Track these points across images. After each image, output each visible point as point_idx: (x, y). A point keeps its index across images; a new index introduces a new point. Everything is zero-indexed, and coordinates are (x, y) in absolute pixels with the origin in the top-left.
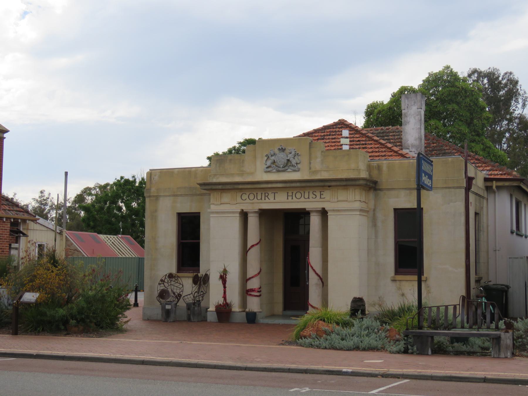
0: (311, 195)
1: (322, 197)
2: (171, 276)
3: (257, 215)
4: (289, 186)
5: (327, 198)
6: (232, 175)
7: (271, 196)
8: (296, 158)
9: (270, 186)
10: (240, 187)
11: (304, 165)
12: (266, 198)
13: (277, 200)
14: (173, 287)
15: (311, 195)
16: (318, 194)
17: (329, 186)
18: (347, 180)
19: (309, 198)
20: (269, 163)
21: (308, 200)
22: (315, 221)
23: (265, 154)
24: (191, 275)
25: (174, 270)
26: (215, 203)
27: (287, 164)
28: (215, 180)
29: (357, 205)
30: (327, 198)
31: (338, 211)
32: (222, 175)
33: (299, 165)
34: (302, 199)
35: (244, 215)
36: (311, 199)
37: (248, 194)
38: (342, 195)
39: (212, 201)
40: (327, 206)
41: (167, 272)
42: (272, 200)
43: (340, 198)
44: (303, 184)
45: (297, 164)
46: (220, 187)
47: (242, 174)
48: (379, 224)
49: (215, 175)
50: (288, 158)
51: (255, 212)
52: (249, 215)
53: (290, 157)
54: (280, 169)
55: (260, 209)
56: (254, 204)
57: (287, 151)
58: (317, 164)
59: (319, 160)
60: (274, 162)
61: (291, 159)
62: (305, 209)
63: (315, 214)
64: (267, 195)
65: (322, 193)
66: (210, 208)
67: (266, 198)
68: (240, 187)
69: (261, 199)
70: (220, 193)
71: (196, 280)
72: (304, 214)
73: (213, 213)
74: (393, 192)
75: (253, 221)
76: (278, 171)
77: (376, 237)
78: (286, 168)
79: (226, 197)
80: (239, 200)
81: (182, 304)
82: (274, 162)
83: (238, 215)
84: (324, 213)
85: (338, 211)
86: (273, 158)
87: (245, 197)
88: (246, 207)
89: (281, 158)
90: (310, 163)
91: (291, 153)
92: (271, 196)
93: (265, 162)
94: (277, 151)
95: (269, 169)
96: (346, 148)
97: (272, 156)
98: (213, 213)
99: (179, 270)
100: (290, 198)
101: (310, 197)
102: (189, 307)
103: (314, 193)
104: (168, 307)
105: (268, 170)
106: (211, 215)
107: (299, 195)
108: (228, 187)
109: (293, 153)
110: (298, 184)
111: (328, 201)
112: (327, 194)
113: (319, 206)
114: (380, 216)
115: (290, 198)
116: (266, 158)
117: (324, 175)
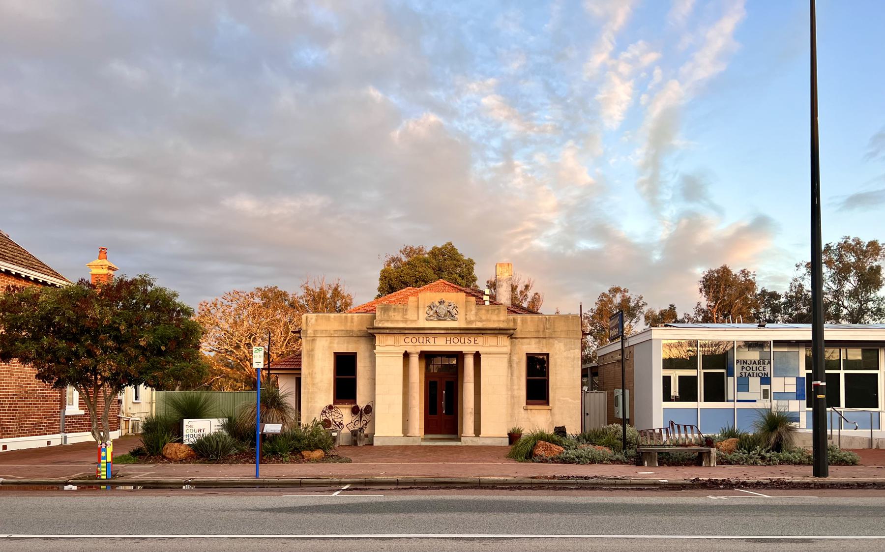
0: (467, 341)
2: (330, 407)
4: (449, 332)
6: (397, 321)
7: (432, 340)
9: (433, 332)
10: (406, 332)
11: (461, 316)
14: (332, 417)
15: (467, 341)
16: (472, 340)
18: (500, 329)
20: (431, 313)
22: (469, 362)
24: (350, 406)
25: (332, 403)
28: (380, 325)
32: (388, 321)
35: (406, 355)
38: (492, 340)
40: (481, 350)
41: (328, 404)
42: (432, 343)
44: (462, 332)
47: (406, 321)
48: (515, 365)
49: (381, 321)
53: (450, 309)
55: (422, 352)
56: (416, 346)
57: (446, 304)
58: (472, 316)
59: (473, 312)
68: (406, 332)
71: (355, 411)
72: (460, 356)
74: (525, 340)
75: (415, 361)
77: (512, 375)
79: (390, 340)
80: (403, 343)
81: (345, 431)
84: (477, 356)
89: (442, 310)
92: (432, 340)
96: (487, 303)
99: (335, 403)
102: (354, 433)
104: (334, 434)
108: (395, 331)
110: (458, 332)
112: (480, 340)
113: (474, 349)
114: (515, 358)
117: (479, 325)
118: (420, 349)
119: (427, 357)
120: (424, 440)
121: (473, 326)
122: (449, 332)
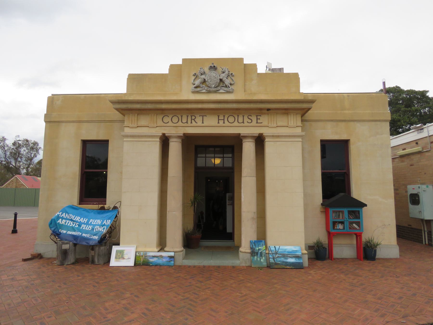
0: (246, 119)
1: (259, 121)
3: (180, 140)
5: (265, 123)
8: (229, 78)
12: (193, 121)
13: (205, 124)
17: (268, 110)
19: (243, 122)
21: (242, 124)
22: (249, 148)
23: (194, 73)
26: (130, 125)
27: (219, 84)
29: (298, 131)
30: (265, 123)
31: (278, 136)
33: (232, 87)
34: (236, 124)
35: (165, 141)
36: (246, 124)
37: (171, 116)
38: (281, 120)
39: (126, 124)
40: (265, 131)
42: (200, 123)
43: (279, 124)
45: (231, 84)
46: (138, 106)
50: (221, 77)
51: (179, 137)
52: (171, 140)
53: (223, 76)
54: (211, 89)
55: (184, 134)
57: (220, 70)
60: (205, 80)
61: (224, 79)
62: (240, 134)
63: (251, 140)
64: (193, 118)
65: (259, 117)
66: (123, 130)
67: (193, 121)
69: (187, 122)
70: (136, 115)
73: (127, 136)
76: (209, 92)
78: (219, 88)
79: (144, 120)
80: (160, 123)
82: (204, 81)
83: (158, 140)
84: (260, 141)
85: (278, 136)
86: (203, 76)
87: (166, 119)
88: (168, 131)
89: (212, 77)
90: (245, 85)
91: (224, 72)
93: (192, 81)
94: (206, 69)
95: (198, 89)
97: (202, 74)
98: (127, 136)
100: (221, 122)
101: (245, 121)
103: (250, 117)
105: (197, 89)
106: (125, 140)
107: (231, 119)
109: (227, 72)
111: (266, 126)
112: (264, 119)
113: (256, 131)
115: (221, 122)
116: (193, 78)
118: (181, 131)
119: (195, 146)
120: (186, 256)
121: (255, 98)
122: (222, 110)
